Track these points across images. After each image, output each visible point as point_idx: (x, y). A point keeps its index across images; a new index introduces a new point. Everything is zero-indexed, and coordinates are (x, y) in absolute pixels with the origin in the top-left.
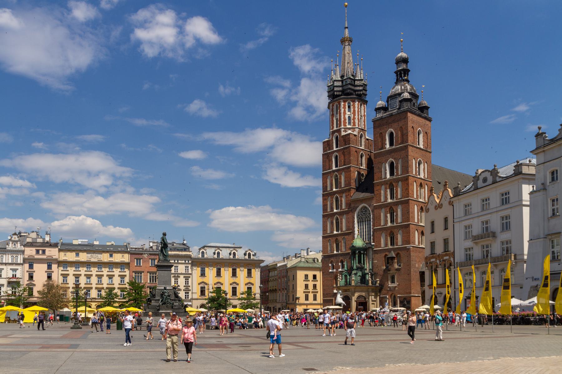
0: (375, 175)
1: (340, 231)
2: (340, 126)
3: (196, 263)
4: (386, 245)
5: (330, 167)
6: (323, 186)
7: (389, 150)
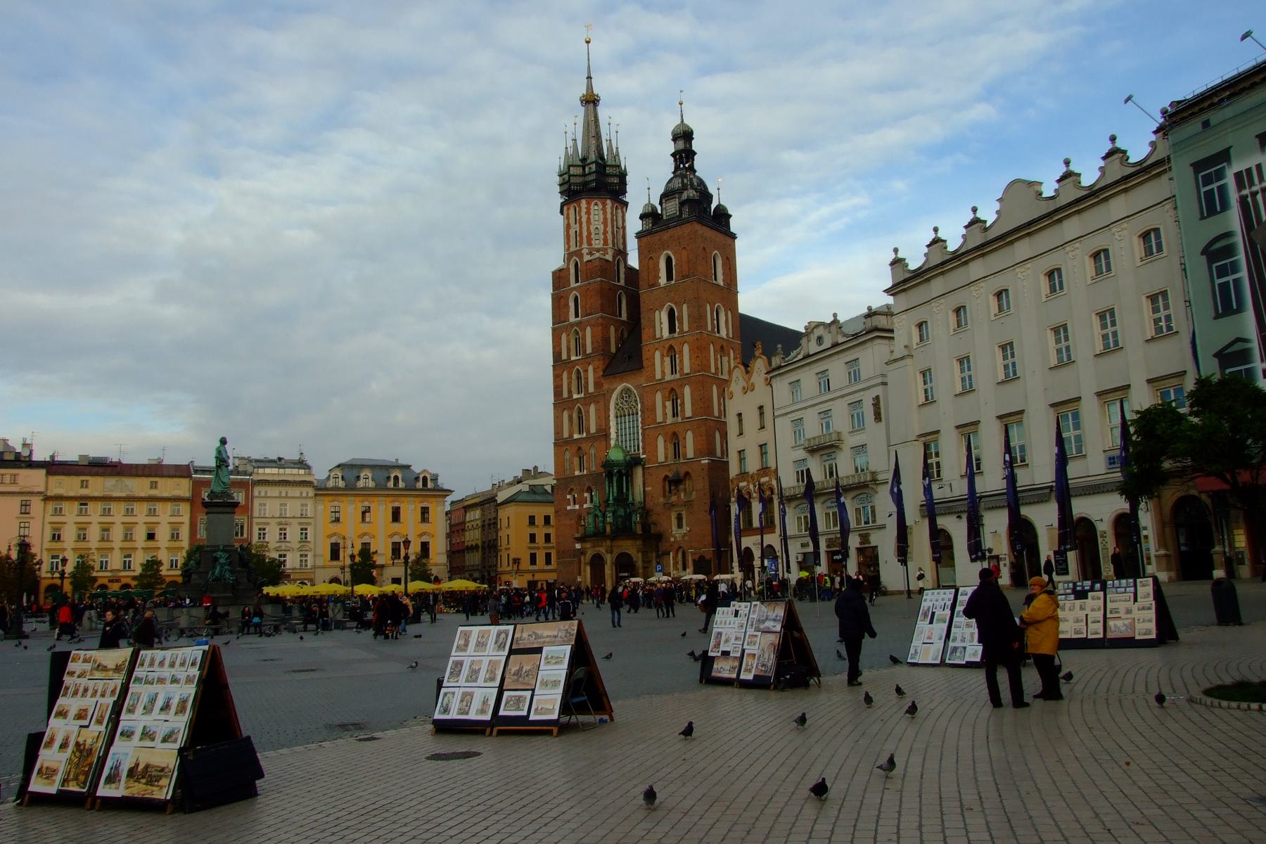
0: (643, 331)
1: (585, 434)
2: (581, 246)
3: (322, 498)
4: (666, 458)
5: (567, 319)
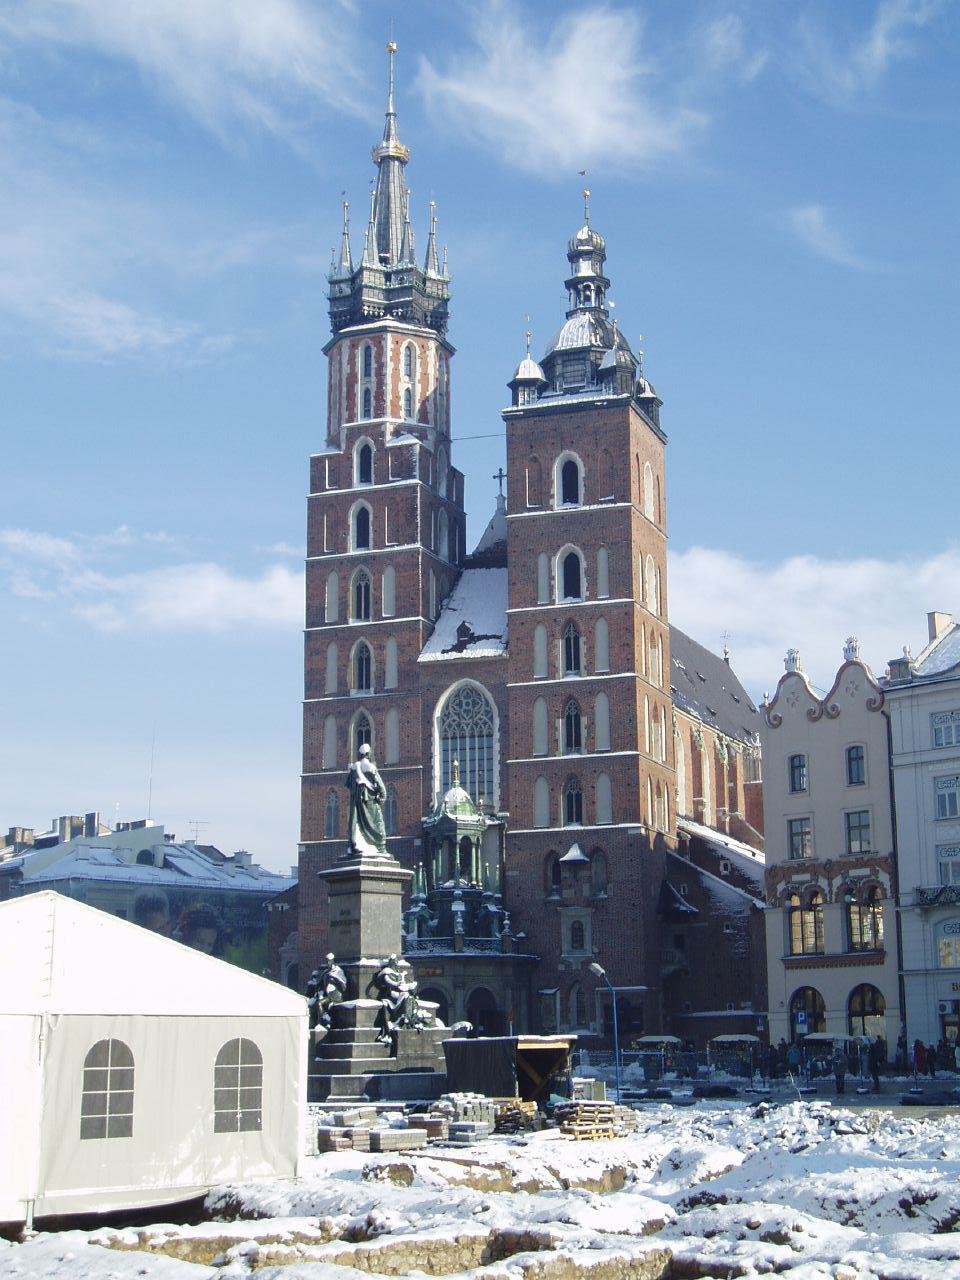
6: (308, 607)
7: (562, 517)
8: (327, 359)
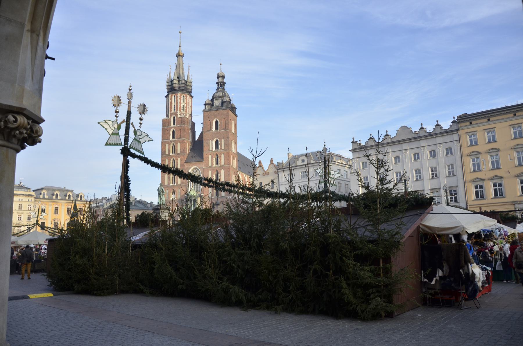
1: (175, 184)
5: (168, 138)
6: (162, 151)
8: (166, 98)
